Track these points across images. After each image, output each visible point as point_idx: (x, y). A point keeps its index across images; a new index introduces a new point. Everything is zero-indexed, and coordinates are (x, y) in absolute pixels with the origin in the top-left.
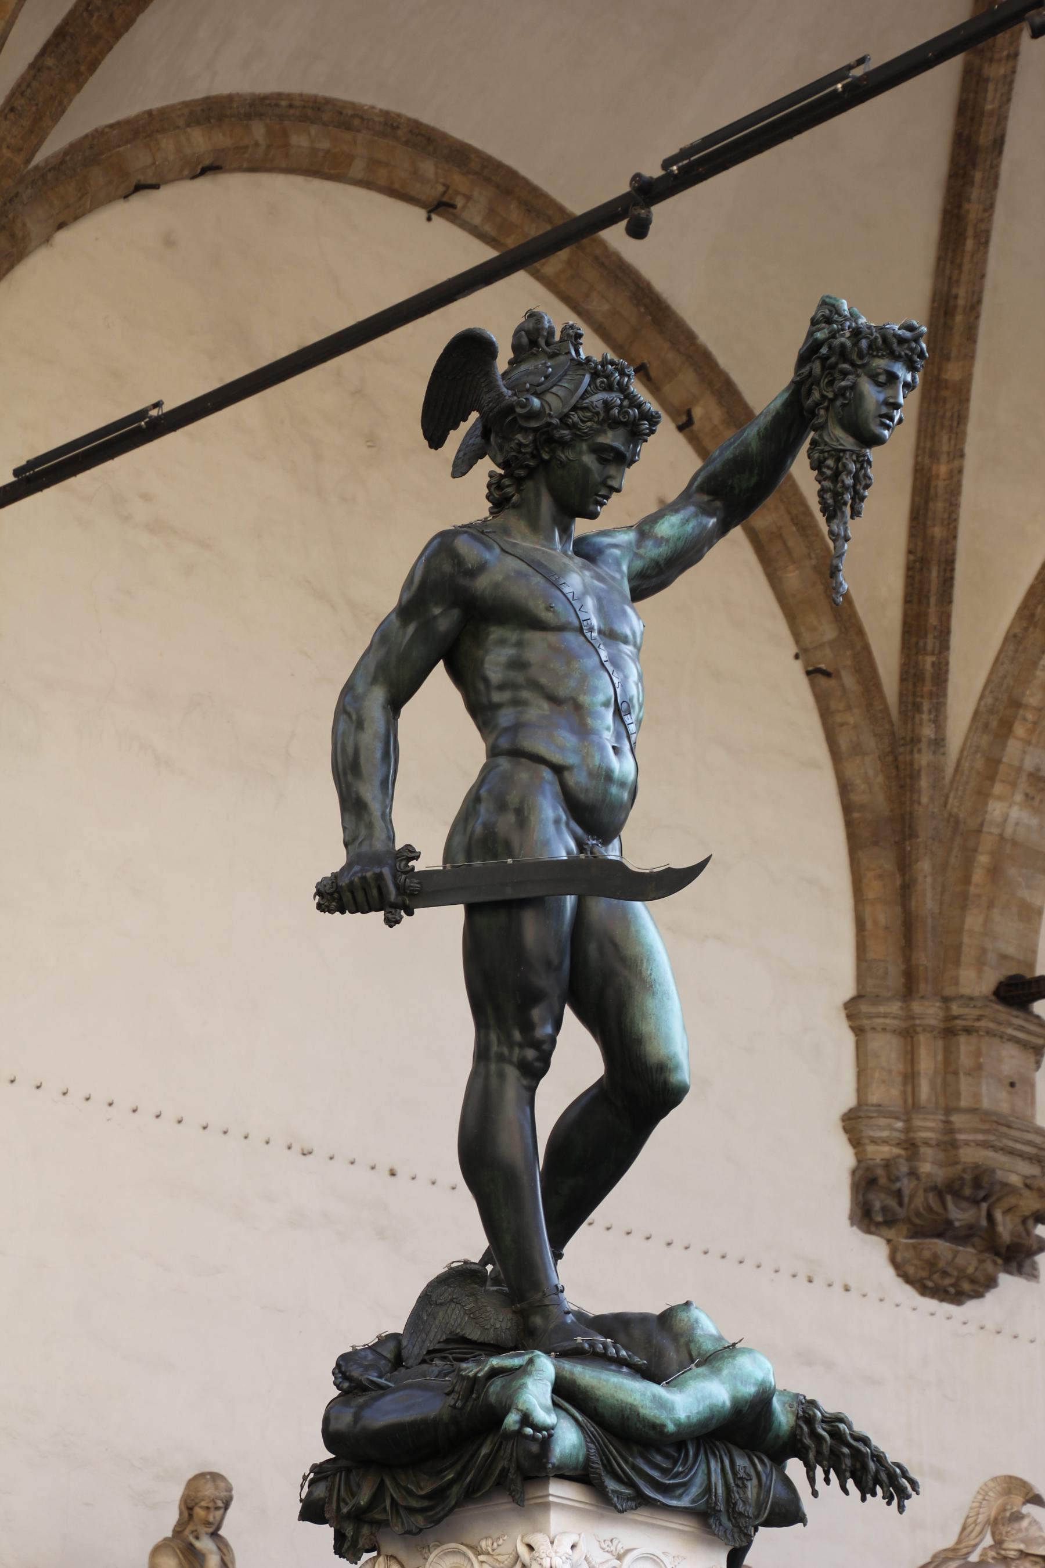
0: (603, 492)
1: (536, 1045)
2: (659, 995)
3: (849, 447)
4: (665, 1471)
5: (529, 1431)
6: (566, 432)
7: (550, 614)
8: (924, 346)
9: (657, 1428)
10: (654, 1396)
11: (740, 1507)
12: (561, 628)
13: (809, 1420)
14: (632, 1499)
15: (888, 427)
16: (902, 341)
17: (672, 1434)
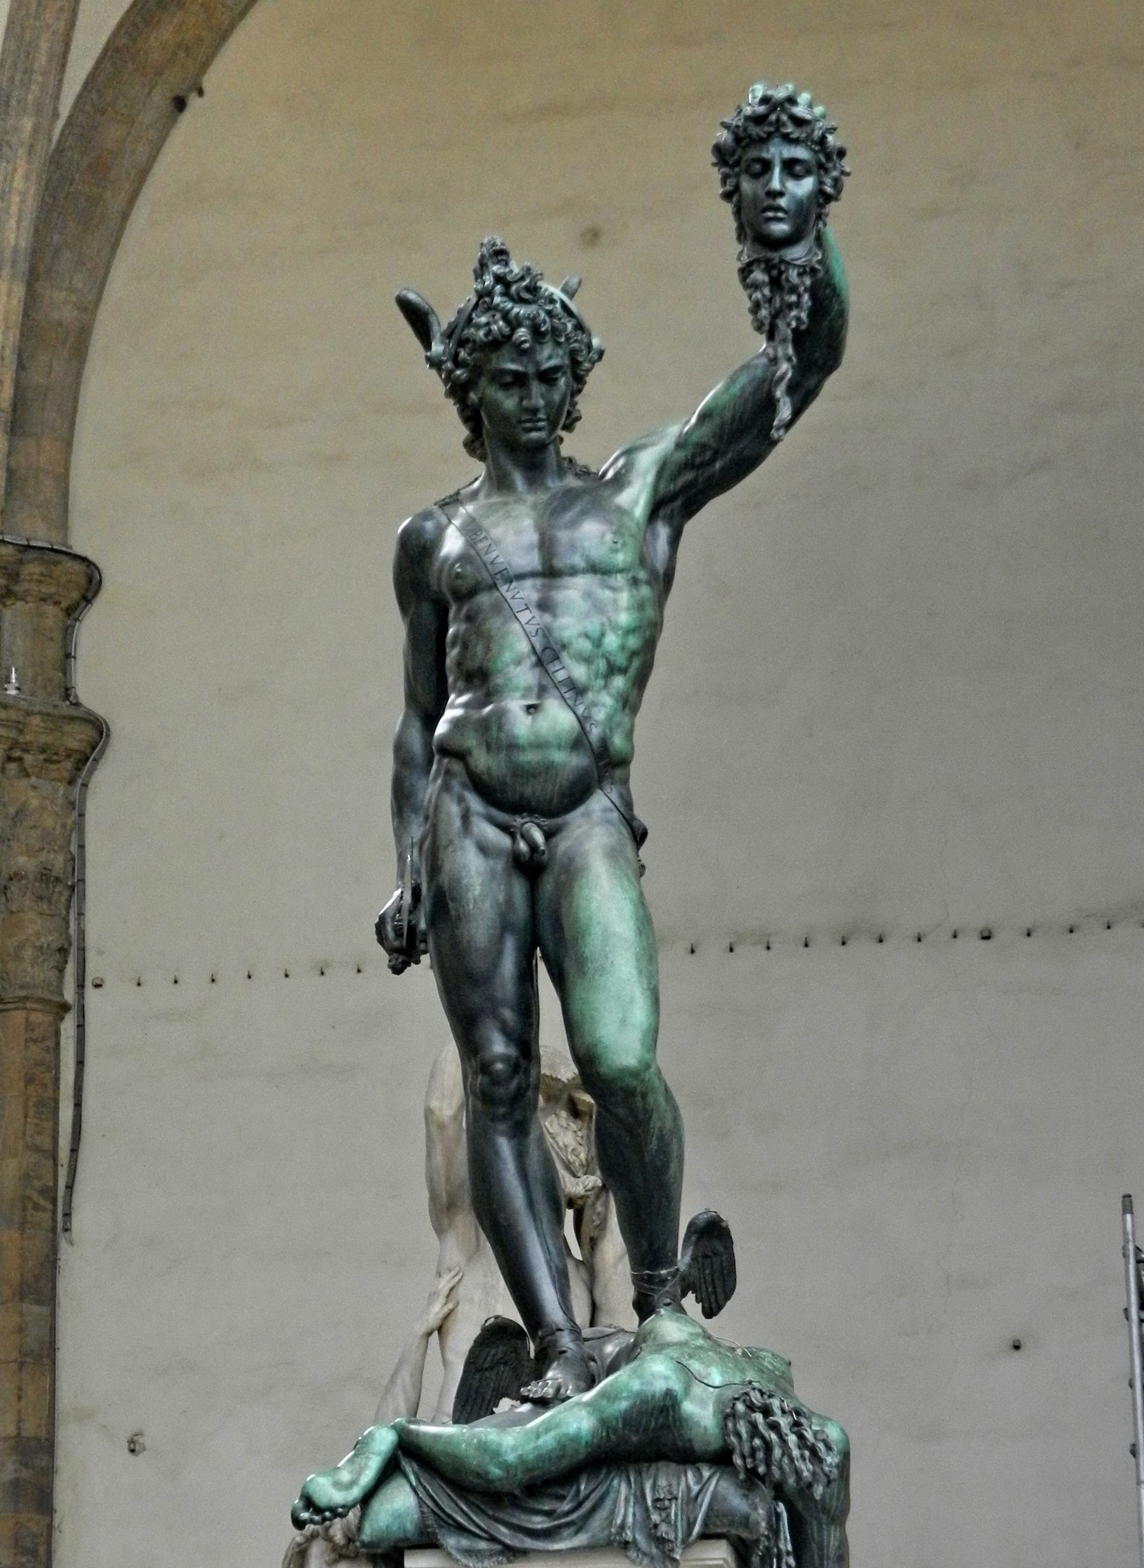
0: (525, 417)
1: (485, 1068)
2: (589, 975)
3: (755, 256)
4: (549, 1514)
5: (305, 1515)
6: (458, 372)
7: (460, 582)
8: (800, 111)
9: (482, 1475)
10: (480, 1441)
11: (663, 1528)
12: (473, 592)
13: (734, 1415)
14: (501, 1553)
15: (779, 220)
16: (759, 120)
17: (500, 1479)
